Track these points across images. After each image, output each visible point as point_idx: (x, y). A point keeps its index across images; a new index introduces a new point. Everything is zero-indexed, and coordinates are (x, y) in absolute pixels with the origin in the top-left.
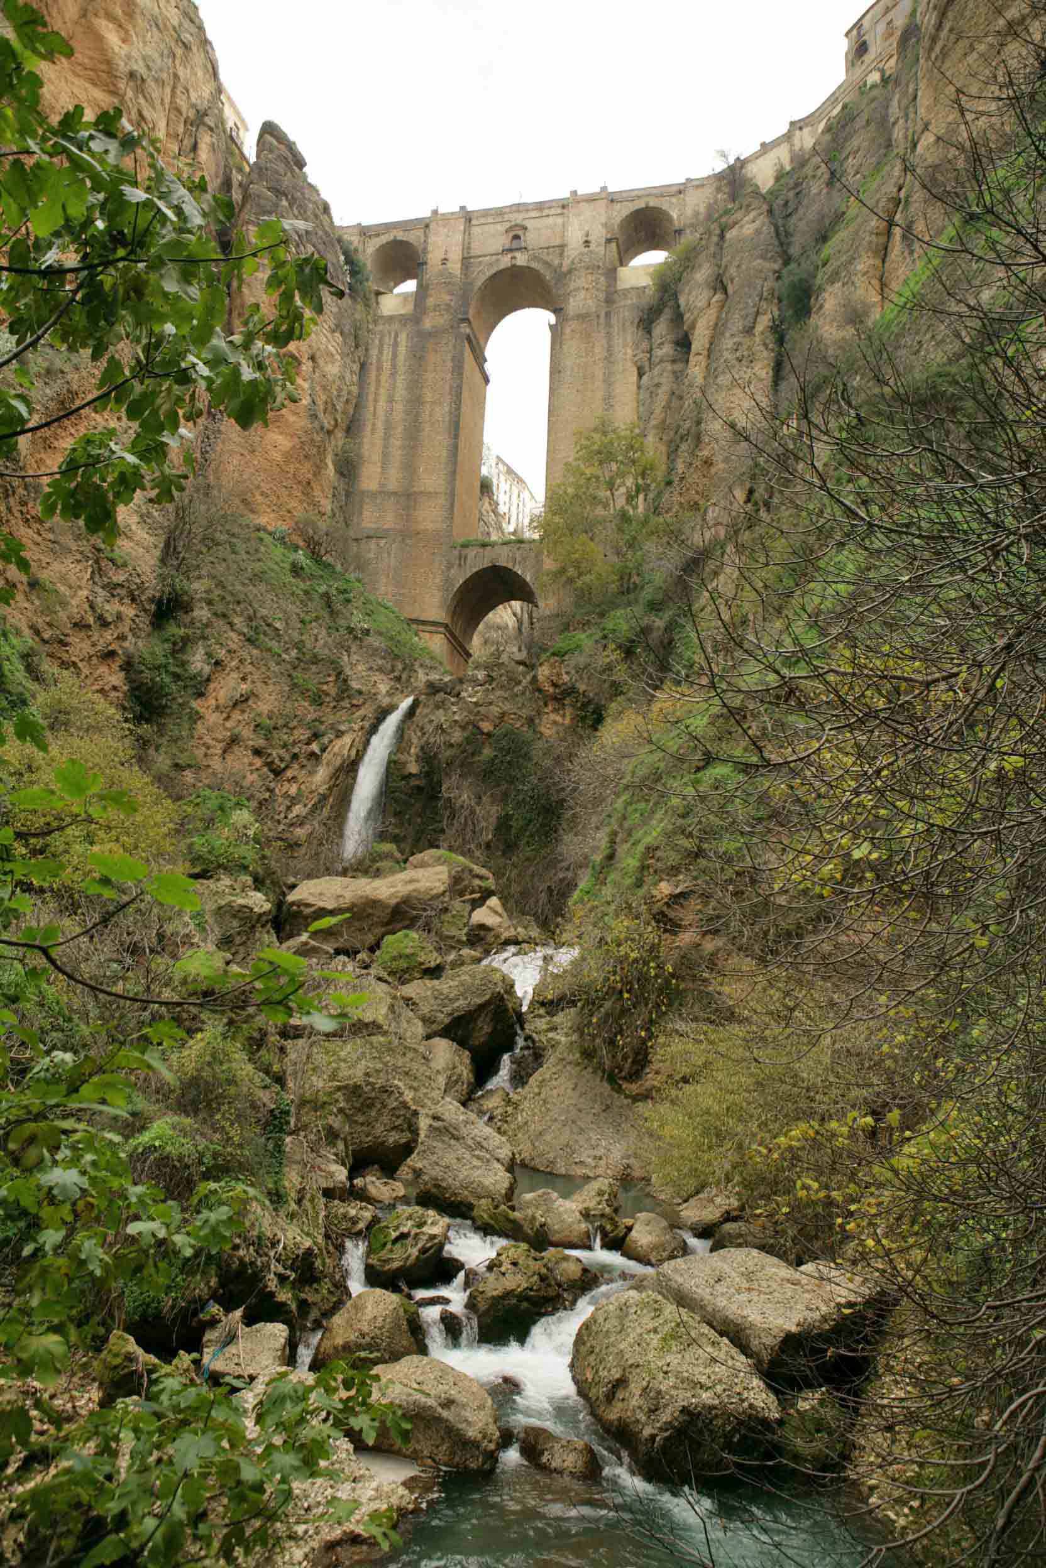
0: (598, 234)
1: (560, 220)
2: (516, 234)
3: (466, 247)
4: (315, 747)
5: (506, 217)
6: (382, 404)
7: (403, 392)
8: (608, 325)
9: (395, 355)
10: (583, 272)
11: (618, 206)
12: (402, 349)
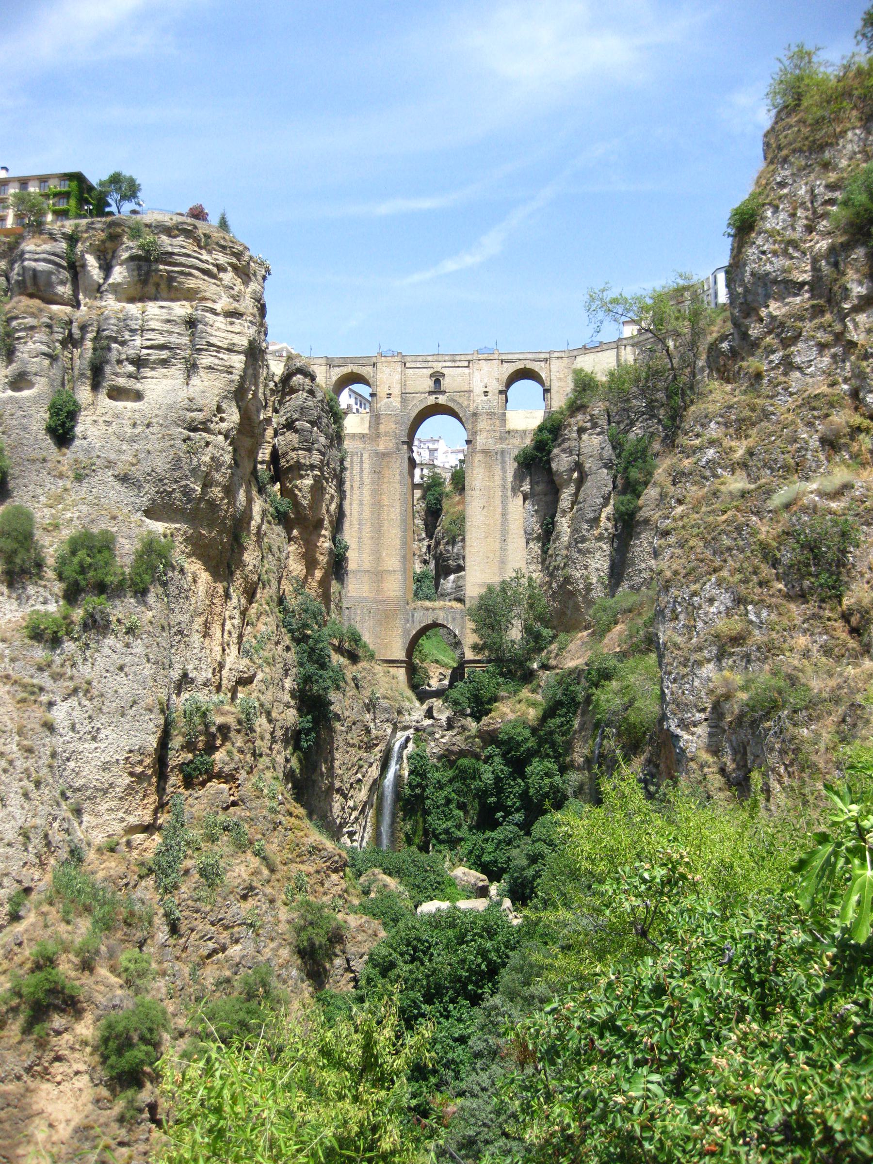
0: (495, 386)
1: (466, 370)
2: (437, 378)
3: (403, 384)
4: (359, 776)
5: (430, 364)
6: (355, 506)
7: (368, 498)
8: (503, 462)
9: (361, 470)
10: (485, 417)
11: (505, 365)
12: (366, 466)
